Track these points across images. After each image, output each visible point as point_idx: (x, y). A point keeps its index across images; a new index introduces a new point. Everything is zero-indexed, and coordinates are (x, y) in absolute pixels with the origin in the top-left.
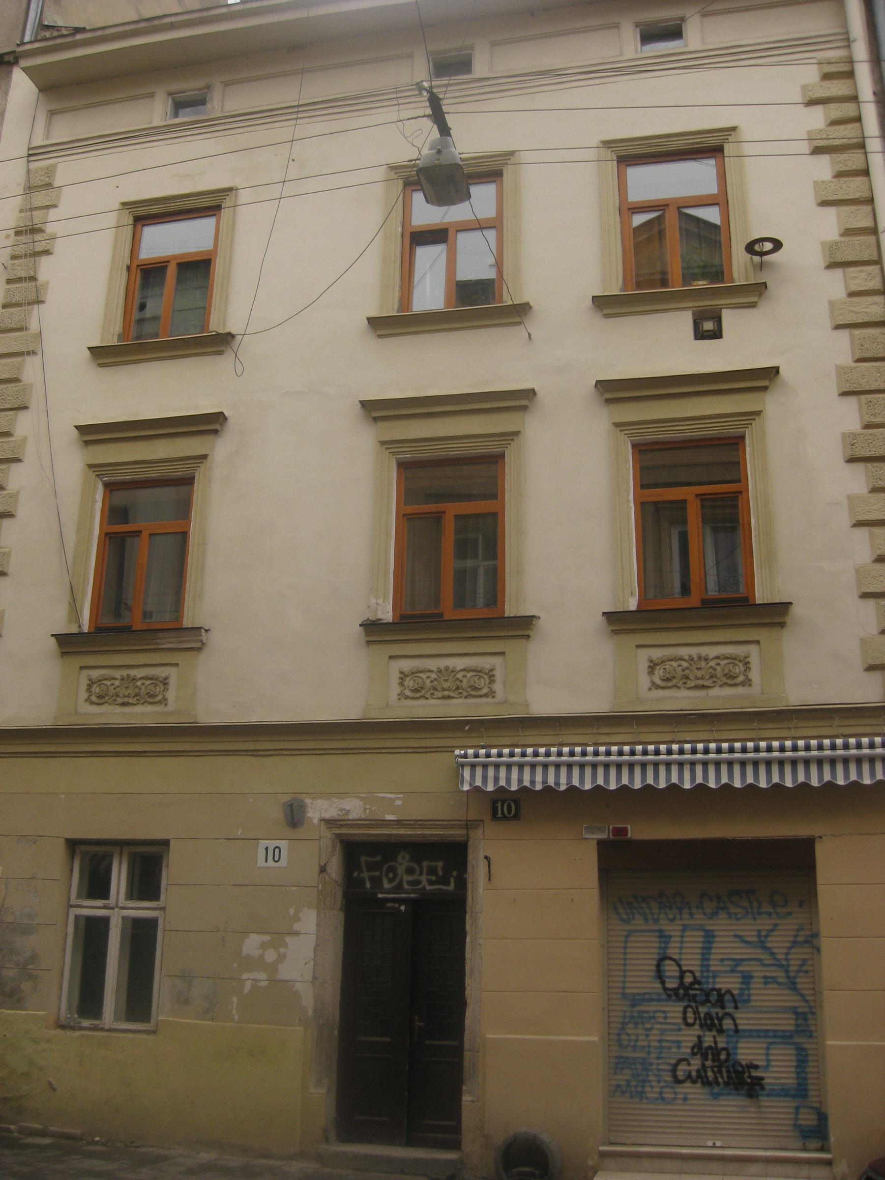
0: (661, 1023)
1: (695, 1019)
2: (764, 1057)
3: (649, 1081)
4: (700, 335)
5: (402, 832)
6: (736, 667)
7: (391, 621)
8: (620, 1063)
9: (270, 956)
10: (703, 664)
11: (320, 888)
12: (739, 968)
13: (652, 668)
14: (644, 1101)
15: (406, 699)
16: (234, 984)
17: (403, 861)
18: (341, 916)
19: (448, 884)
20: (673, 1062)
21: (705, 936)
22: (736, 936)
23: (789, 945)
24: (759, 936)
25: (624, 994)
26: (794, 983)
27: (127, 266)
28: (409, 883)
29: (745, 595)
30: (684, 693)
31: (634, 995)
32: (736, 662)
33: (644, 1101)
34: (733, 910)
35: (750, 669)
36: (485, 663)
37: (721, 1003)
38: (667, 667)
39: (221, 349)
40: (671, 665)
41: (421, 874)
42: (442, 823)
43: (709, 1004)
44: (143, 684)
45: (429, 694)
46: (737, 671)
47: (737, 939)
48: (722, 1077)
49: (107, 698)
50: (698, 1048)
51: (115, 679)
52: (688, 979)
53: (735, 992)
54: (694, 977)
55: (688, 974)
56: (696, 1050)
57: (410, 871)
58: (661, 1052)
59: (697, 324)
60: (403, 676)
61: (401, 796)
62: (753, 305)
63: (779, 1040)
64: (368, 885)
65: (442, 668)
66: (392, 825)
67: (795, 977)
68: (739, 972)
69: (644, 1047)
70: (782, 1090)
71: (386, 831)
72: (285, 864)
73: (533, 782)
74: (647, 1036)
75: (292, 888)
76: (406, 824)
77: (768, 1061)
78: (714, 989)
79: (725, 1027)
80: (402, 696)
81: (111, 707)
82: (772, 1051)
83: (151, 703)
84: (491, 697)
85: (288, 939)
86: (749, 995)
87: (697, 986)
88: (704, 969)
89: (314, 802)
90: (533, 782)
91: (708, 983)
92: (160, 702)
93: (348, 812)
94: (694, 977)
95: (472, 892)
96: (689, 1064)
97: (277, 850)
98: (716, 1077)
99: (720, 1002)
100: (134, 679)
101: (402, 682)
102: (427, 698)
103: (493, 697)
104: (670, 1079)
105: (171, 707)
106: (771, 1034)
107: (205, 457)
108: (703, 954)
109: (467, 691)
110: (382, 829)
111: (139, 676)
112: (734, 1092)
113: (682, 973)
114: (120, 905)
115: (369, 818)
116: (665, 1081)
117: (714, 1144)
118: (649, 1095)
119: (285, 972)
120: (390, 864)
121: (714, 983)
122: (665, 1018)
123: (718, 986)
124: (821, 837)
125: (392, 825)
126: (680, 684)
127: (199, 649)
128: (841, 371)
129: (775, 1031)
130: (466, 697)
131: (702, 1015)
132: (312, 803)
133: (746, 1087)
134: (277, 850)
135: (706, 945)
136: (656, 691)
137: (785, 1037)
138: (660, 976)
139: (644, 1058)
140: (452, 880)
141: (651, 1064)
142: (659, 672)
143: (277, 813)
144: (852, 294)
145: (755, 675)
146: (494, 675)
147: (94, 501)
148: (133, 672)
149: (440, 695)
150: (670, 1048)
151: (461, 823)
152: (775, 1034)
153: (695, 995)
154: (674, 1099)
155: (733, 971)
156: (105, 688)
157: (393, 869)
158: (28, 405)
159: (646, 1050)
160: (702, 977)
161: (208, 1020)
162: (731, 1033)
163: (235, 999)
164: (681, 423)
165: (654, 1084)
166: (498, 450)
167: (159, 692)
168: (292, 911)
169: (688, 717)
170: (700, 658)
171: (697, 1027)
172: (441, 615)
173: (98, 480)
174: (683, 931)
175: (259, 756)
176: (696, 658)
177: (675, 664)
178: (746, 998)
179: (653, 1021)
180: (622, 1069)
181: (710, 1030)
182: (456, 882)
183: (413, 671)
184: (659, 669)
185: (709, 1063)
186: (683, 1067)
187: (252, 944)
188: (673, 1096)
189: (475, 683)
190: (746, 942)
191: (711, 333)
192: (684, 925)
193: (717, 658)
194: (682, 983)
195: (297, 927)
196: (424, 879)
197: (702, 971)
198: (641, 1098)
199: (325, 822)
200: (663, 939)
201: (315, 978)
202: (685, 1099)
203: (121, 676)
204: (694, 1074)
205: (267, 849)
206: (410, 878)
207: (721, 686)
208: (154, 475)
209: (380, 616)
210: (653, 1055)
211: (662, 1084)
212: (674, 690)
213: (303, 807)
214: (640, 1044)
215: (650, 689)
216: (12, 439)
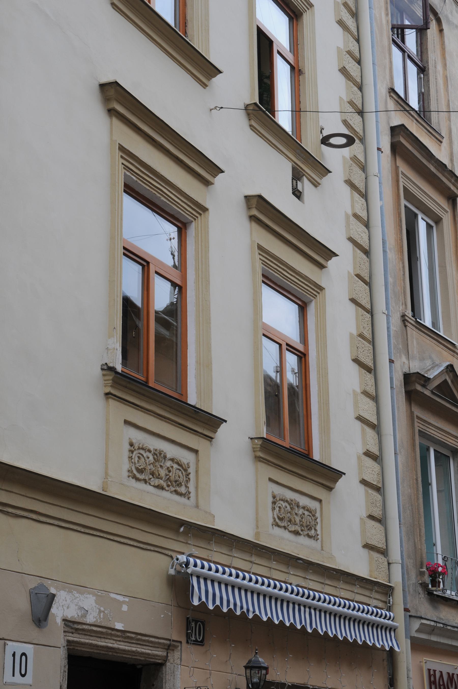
5: (123, 646)
29: (306, 452)
30: (286, 535)
110: (107, 641)
125: (118, 636)
144: (356, 216)
169: (298, 561)
191: (298, 194)
205: (14, 655)
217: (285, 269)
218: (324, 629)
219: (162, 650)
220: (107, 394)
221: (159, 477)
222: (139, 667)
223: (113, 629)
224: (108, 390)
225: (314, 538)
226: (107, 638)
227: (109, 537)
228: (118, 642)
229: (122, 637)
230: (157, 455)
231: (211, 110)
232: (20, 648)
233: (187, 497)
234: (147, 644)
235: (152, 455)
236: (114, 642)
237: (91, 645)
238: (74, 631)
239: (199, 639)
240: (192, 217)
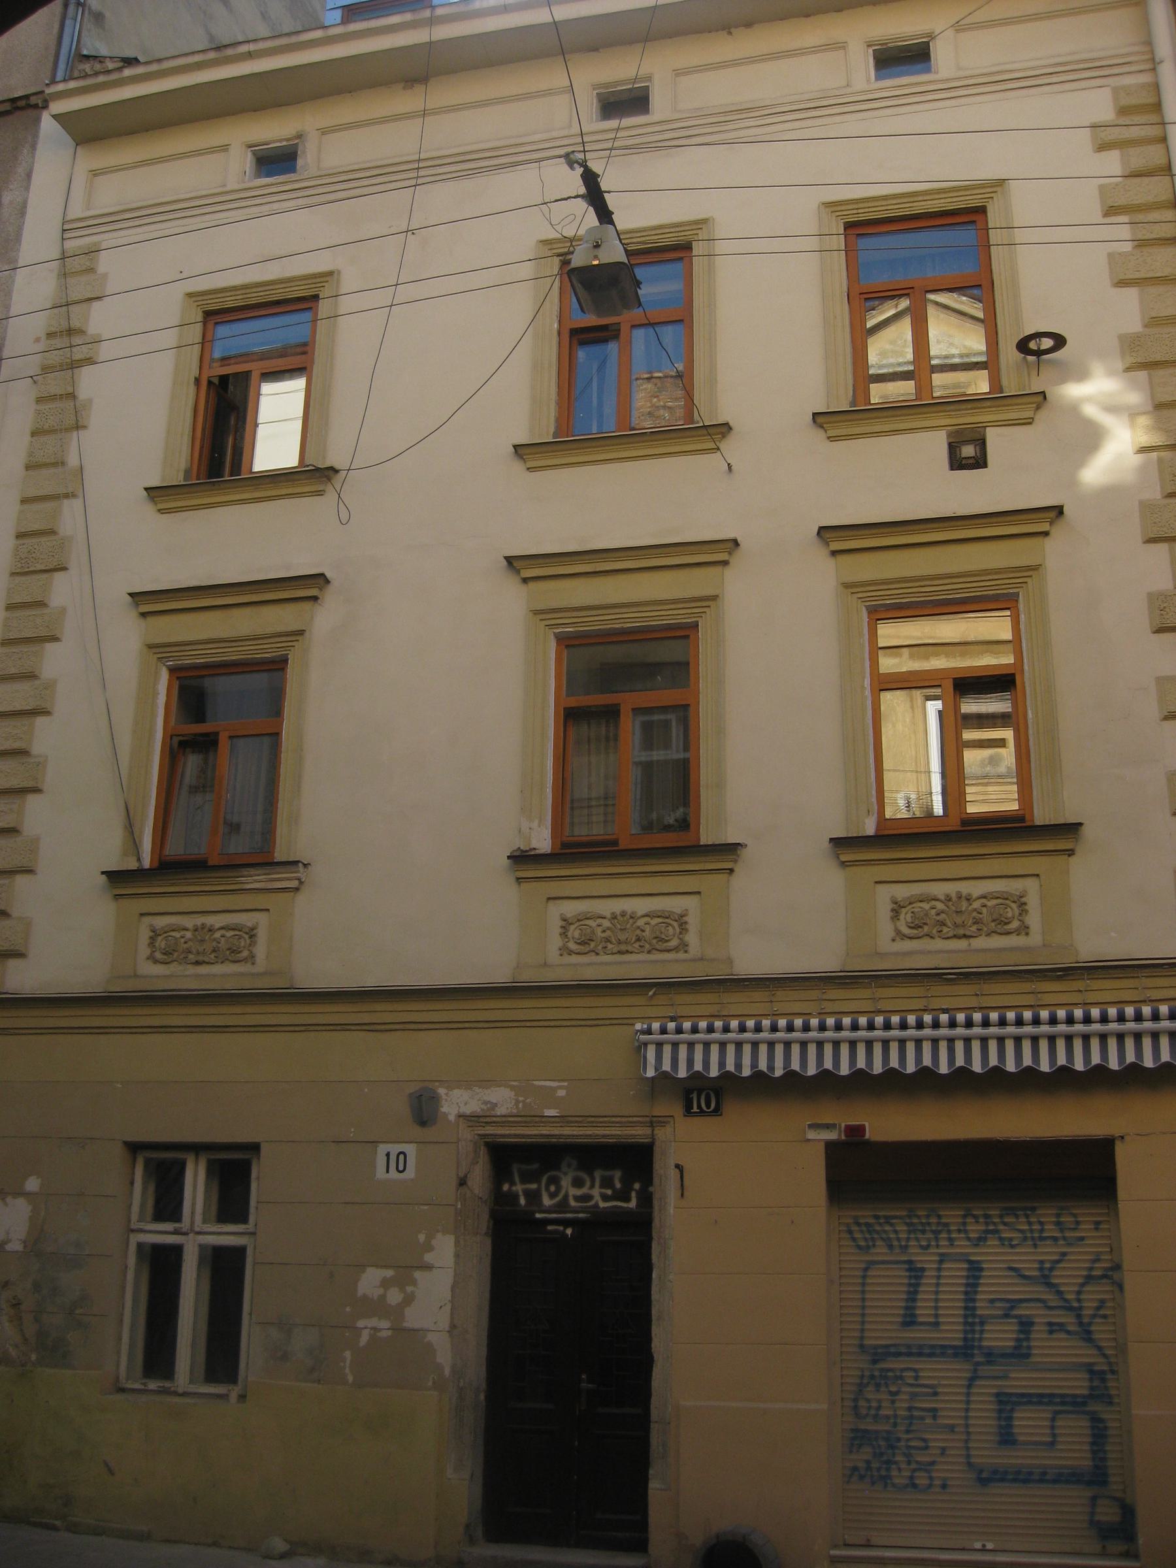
0: (912, 1385)
3: (896, 1463)
4: (957, 463)
5: (567, 1131)
6: (1009, 909)
7: (549, 852)
8: (858, 1438)
9: (394, 1297)
10: (964, 904)
12: (1015, 1312)
13: (897, 912)
15: (570, 954)
18: (488, 1242)
19: (628, 1200)
23: (1080, 1281)
25: (862, 1346)
26: (1089, 1332)
27: (195, 378)
28: (577, 1198)
30: (939, 944)
31: (876, 1347)
32: (1007, 902)
35: (1027, 911)
36: (675, 905)
38: (916, 910)
40: (921, 908)
41: (592, 1186)
42: (618, 1119)
44: (223, 936)
45: (600, 947)
46: (1010, 915)
49: (176, 954)
51: (187, 930)
57: (578, 1183)
58: (911, 1424)
59: (953, 448)
60: (566, 923)
61: (566, 1084)
62: (1029, 422)
64: (522, 1201)
65: (618, 913)
67: (1090, 1324)
68: (1016, 1317)
69: (888, 1417)
71: (545, 1131)
73: (738, 1066)
74: (893, 1402)
75: (422, 1207)
76: (572, 1122)
77: (1054, 1435)
80: (565, 950)
82: (1058, 1423)
84: (682, 951)
85: (417, 1274)
86: (1029, 1347)
89: (451, 1093)
90: (738, 1066)
92: (245, 960)
93: (494, 1106)
97: (402, 1157)
100: (210, 930)
101: (564, 933)
102: (597, 954)
103: (686, 952)
107: (301, 633)
108: (966, 1293)
111: (217, 926)
114: (197, 1229)
115: (523, 1114)
117: (984, 1546)
118: (897, 1481)
119: (414, 1318)
122: (916, 1378)
124: (1122, 1137)
125: (553, 1122)
127: (297, 889)
128: (1146, 508)
130: (649, 952)
132: (447, 1094)
134: (402, 1157)
137: (1074, 1404)
139: (888, 1432)
140: (633, 1194)
141: (899, 1440)
142: (906, 916)
145: (1034, 919)
146: (686, 923)
147: (155, 694)
148: (210, 920)
149: (615, 950)
152: (1064, 1400)
154: (930, 1486)
155: (1006, 1316)
157: (555, 1181)
158: (66, 566)
159: (892, 1421)
163: (348, 1354)
165: (903, 1466)
167: (244, 947)
168: (422, 1237)
170: (960, 897)
173: (159, 663)
174: (941, 1262)
176: (954, 898)
177: (926, 906)
178: (1025, 1351)
180: (860, 1446)
182: (638, 1198)
183: (579, 918)
184: (906, 914)
187: (370, 1281)
188: (927, 1482)
189: (661, 933)
193: (984, 897)
195: (428, 1258)
196: (596, 1192)
198: (886, 1486)
200: (913, 1274)
201: (453, 1326)
202: (944, 1486)
203: (194, 926)
205: (388, 1155)
206: (579, 1192)
207: (988, 935)
208: (234, 658)
210: (901, 1428)
211: (914, 1466)
212: (926, 940)
213: (434, 1099)
214: (883, 1412)
215: (893, 940)
216: (46, 611)
223: (544, 1116)
227: (528, 1024)
229: (563, 1122)
232: (395, 1149)
233: (682, 951)
235: (609, 920)
238: (484, 1125)
239: (708, 1108)
240: (694, 617)
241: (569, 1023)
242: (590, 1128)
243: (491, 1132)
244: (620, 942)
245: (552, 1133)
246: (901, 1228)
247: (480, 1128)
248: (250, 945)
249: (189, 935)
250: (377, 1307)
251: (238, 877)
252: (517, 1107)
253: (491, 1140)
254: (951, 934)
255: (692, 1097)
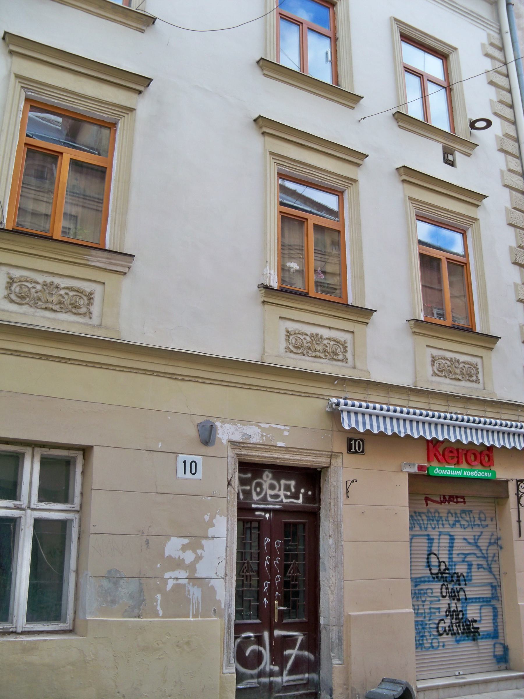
1: (447, 593)
2: (479, 615)
3: (425, 636)
4: (447, 161)
5: (287, 456)
9: (189, 557)
11: (229, 498)
12: (467, 559)
14: (423, 650)
15: (291, 353)
16: (158, 583)
17: (267, 479)
19: (298, 498)
20: (437, 622)
21: (450, 539)
22: (465, 539)
23: (487, 544)
24: (474, 539)
26: (490, 568)
28: (271, 496)
29: (470, 327)
30: (448, 381)
33: (423, 650)
34: (463, 522)
37: (458, 582)
38: (441, 363)
39: (144, 28)
43: (453, 583)
47: (464, 541)
48: (460, 629)
50: (450, 613)
52: (443, 567)
53: (465, 574)
54: (446, 565)
55: (442, 564)
56: (448, 613)
57: (272, 487)
58: (431, 616)
61: (288, 428)
63: (485, 604)
66: (281, 450)
67: (491, 564)
68: (467, 562)
69: (422, 613)
70: (488, 634)
72: (201, 477)
73: (386, 429)
74: (423, 605)
76: (291, 451)
77: (481, 617)
78: (455, 573)
79: (460, 597)
80: (288, 350)
81: (32, 310)
82: (483, 611)
83: (75, 314)
84: (345, 362)
85: (204, 542)
87: (447, 571)
88: (450, 560)
89: (224, 426)
91: (452, 569)
92: (84, 314)
94: (446, 565)
95: (335, 505)
96: (445, 623)
97: (193, 464)
98: (458, 630)
99: (458, 582)
102: (304, 355)
103: (347, 362)
104: (435, 633)
105: (95, 320)
106: (481, 600)
108: (449, 550)
109: (330, 355)
110: (272, 453)
111: (62, 286)
112: (467, 638)
113: (440, 562)
114: (32, 506)
115: (265, 443)
116: (433, 635)
117: (459, 673)
118: (426, 645)
119: (202, 571)
120: (258, 480)
121: (455, 569)
123: (457, 571)
125: (281, 450)
126: (447, 375)
129: (483, 598)
130: (329, 359)
131: (450, 590)
133: (472, 634)
134: (193, 464)
135: (451, 545)
136: (435, 377)
138: (429, 565)
139: (422, 621)
140: (301, 495)
141: (426, 624)
142: (436, 365)
143: (193, 432)
144: (510, 170)
148: (57, 281)
149: (314, 355)
150: (435, 613)
151: (327, 453)
153: (446, 577)
154: (438, 646)
155: (463, 561)
156: (27, 289)
157: (259, 485)
159: (423, 615)
160: (449, 565)
161: (135, 617)
162: (464, 601)
163: (159, 596)
164: (441, 211)
165: (428, 638)
166: (342, 188)
168: (207, 518)
169: (455, 397)
171: (447, 598)
172: (308, 293)
174: (440, 535)
175: (176, 379)
177: (444, 362)
178: (469, 578)
179: (426, 595)
181: (454, 600)
182: (303, 498)
185: (454, 621)
186: (442, 625)
188: (437, 644)
190: (469, 543)
191: (450, 163)
192: (440, 532)
193: (464, 363)
194: (440, 570)
196: (282, 493)
197: (449, 562)
198: (422, 649)
199: (231, 443)
200: (430, 541)
202: (444, 646)
204: (447, 629)
205: (185, 462)
206: (272, 493)
208: (81, 108)
209: (272, 284)
210: (427, 618)
211: (432, 637)
215: (432, 375)
217: (438, 210)
218: (481, 441)
219: (325, 458)
220: (264, 302)
221: (316, 351)
222: (319, 470)
224: (262, 300)
225: (477, 381)
226: (272, 452)
227: (269, 390)
228: (283, 454)
230: (313, 337)
231: (359, 121)
232: (189, 458)
233: (345, 362)
234: (310, 455)
236: (280, 454)
237: (258, 456)
238: (241, 448)
239: (359, 450)
241: (291, 393)
242: (299, 456)
243: (245, 453)
244: (316, 351)
245: (279, 457)
246: (425, 518)
247: (238, 450)
248: (88, 304)
249: (39, 287)
250: (178, 564)
251: (86, 255)
252: (263, 439)
253: (242, 458)
254: (453, 377)
255: (352, 443)
